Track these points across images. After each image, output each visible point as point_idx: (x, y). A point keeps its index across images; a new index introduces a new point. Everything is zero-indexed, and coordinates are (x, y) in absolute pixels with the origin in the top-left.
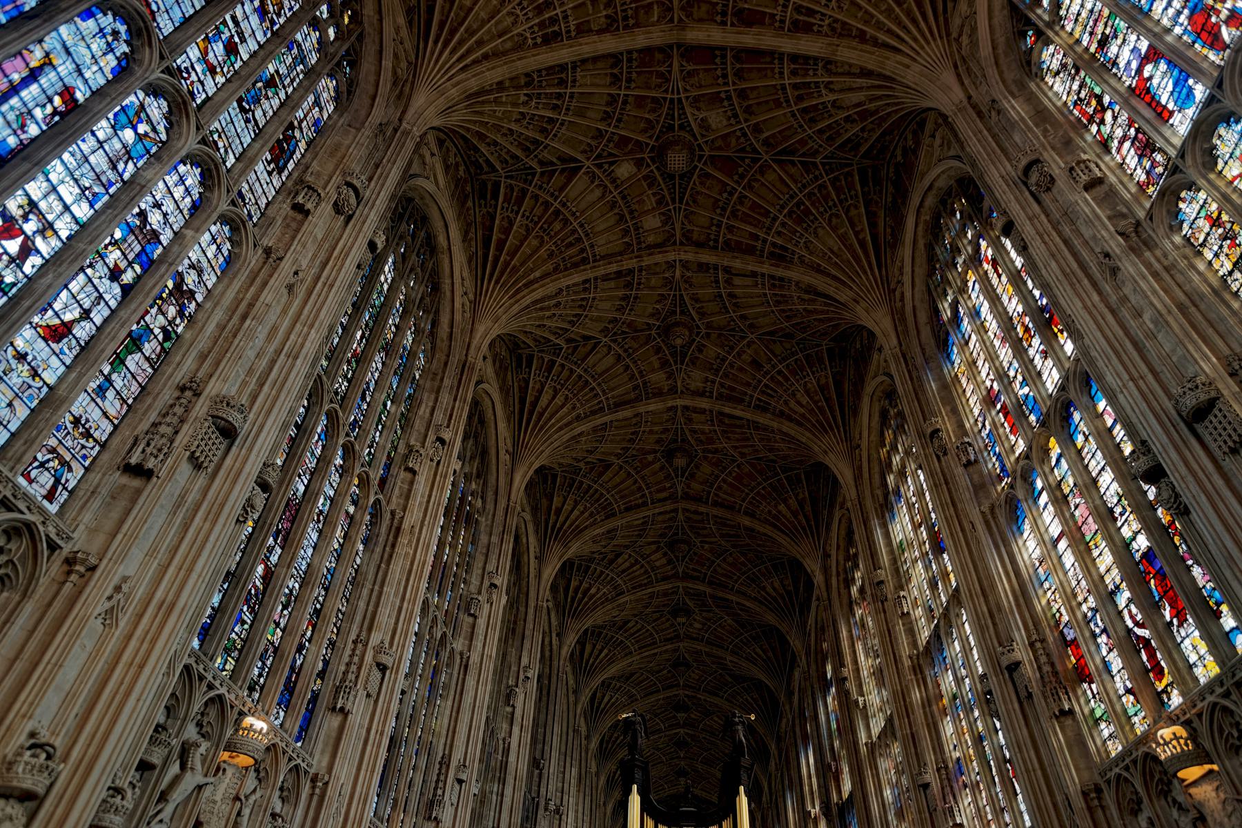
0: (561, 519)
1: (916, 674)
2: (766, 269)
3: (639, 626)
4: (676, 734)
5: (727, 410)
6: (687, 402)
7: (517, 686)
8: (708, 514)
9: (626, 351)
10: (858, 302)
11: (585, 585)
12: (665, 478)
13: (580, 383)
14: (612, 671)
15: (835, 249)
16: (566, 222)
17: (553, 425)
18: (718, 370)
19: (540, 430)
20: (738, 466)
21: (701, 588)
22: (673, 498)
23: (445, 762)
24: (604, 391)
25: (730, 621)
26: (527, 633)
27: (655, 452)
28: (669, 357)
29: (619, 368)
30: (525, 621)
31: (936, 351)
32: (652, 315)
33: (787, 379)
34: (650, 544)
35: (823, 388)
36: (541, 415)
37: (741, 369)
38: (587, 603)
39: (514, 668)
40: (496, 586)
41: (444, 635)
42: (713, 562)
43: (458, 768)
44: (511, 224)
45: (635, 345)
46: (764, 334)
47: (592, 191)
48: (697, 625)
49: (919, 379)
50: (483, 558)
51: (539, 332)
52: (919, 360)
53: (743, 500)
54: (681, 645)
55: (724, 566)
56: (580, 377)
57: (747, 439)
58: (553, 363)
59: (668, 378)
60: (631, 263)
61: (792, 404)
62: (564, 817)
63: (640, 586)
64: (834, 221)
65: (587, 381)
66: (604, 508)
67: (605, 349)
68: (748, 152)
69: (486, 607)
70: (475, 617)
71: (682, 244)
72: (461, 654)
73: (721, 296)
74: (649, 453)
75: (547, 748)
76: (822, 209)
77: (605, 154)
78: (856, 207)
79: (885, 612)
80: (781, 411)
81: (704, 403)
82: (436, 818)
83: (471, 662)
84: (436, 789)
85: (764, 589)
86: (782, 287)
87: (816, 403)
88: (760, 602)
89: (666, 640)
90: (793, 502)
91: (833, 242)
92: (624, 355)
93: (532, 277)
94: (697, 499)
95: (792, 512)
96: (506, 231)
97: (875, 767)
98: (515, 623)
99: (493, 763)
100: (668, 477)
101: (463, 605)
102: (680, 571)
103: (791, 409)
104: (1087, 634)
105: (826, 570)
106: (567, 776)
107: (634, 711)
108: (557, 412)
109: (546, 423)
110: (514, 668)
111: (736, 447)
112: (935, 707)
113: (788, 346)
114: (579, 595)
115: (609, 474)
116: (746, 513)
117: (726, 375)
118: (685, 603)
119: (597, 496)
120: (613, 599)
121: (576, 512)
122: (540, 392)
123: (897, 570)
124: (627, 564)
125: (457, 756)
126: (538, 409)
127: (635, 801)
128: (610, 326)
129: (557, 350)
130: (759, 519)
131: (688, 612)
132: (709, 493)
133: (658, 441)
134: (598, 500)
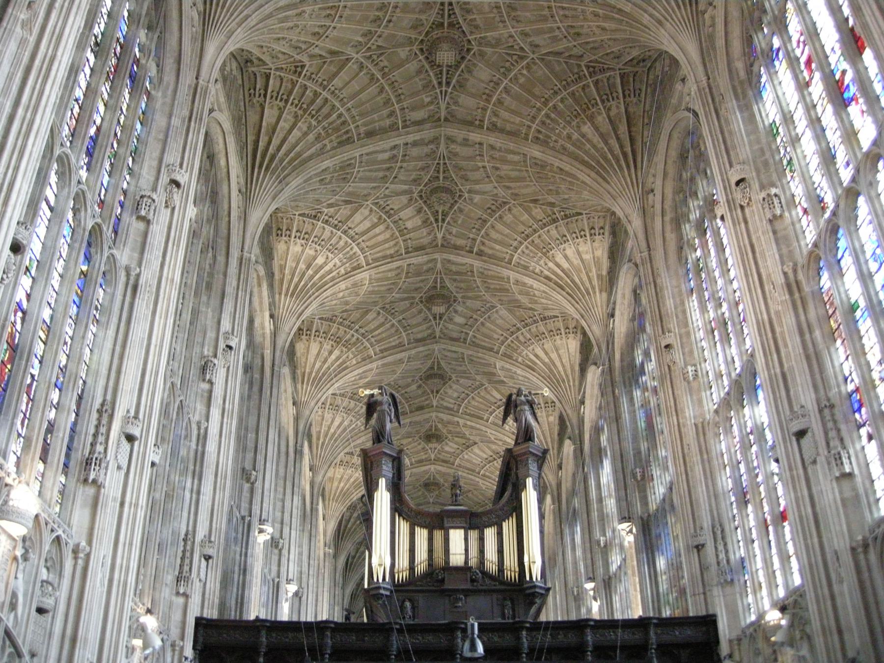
0: (275, 142)
1: (791, 293)
3: (381, 319)
4: (426, 472)
7: (215, 356)
8: (481, 144)
11: (310, 252)
12: (425, 87)
20: (528, 67)
22: (435, 120)
23: (106, 411)
25: (504, 312)
26: (230, 290)
27: (410, 42)
30: (225, 275)
38: (312, 277)
39: (211, 335)
40: (178, 184)
41: (96, 231)
42: (485, 221)
43: (126, 420)
48: (459, 320)
50: (159, 146)
53: (534, 118)
54: (436, 347)
55: (499, 226)
57: (544, 19)
62: (285, 552)
63: (385, 257)
66: (337, 130)
69: (165, 214)
70: (148, 222)
72: (128, 270)
74: (402, 45)
75: (260, 458)
79: (746, 222)
82: (94, 481)
83: (142, 281)
84: (93, 445)
89: (418, 341)
90: (601, 119)
94: (469, 123)
95: (602, 136)
97: (704, 450)
98: (211, 275)
99: (183, 452)
100: (427, 86)
101: (128, 204)
102: (440, 236)
106: (288, 504)
107: (380, 388)
110: (211, 335)
111: (526, 35)
112: (817, 333)
115: (344, 75)
119: (325, 110)
120: (347, 275)
121: (296, 133)
123: (766, 164)
124: (367, 224)
125: (125, 404)
127: (383, 499)
130: (553, 149)
132: (484, 109)
133: (414, 27)
134: (328, 115)
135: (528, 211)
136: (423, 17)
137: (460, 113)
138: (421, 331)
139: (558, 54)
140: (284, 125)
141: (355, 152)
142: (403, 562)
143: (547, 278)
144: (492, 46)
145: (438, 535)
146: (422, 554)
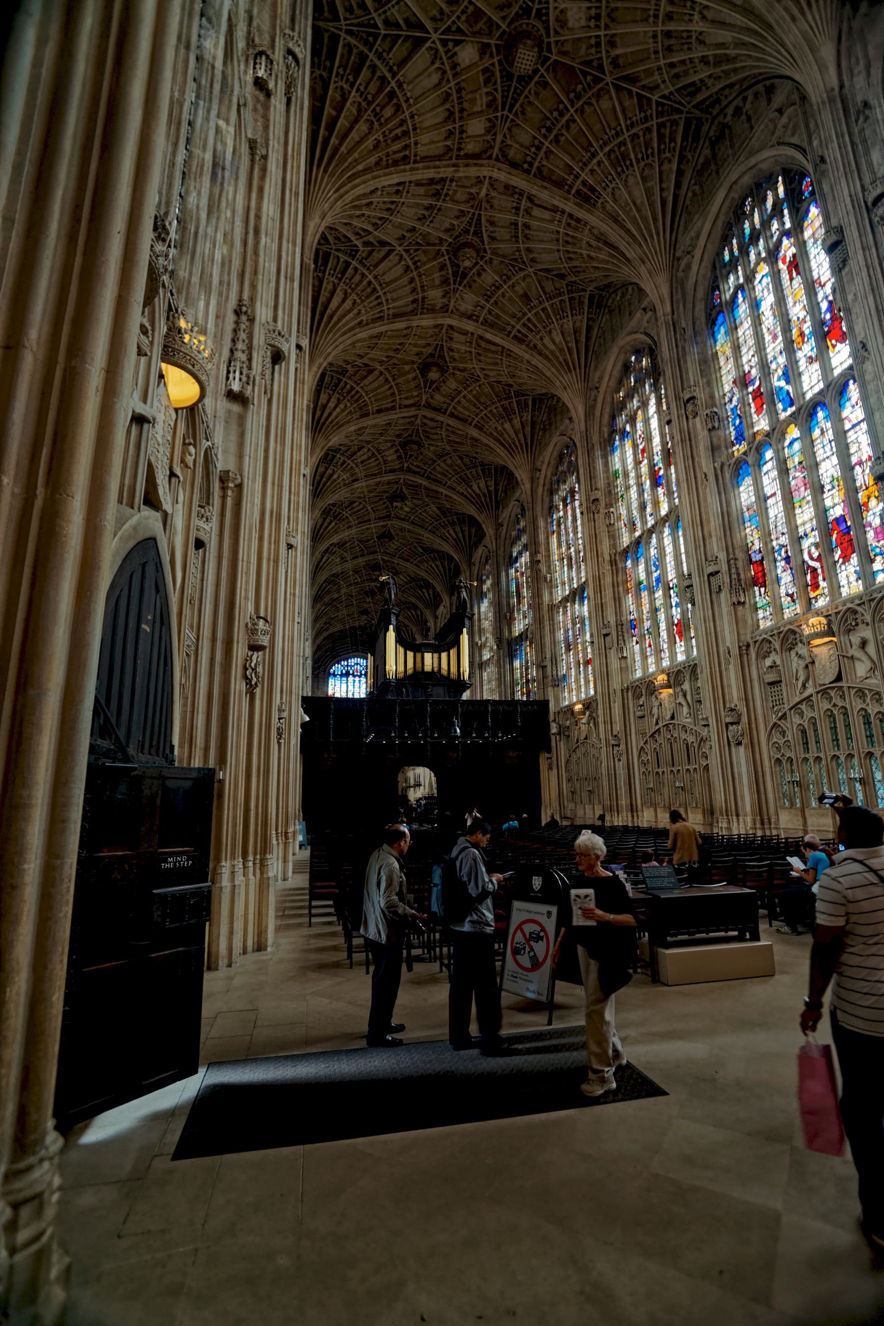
0: (325, 415)
2: (570, 207)
5: (488, 336)
6: (454, 322)
9: (415, 263)
10: (644, 263)
13: (369, 290)
14: (335, 539)
15: (638, 202)
16: (398, 107)
17: (340, 329)
18: (490, 297)
19: (330, 331)
21: (420, 481)
24: (387, 300)
25: (434, 509)
27: (413, 362)
28: (450, 276)
29: (406, 280)
31: (704, 326)
32: (447, 230)
33: (548, 317)
34: (386, 441)
35: (576, 332)
36: (331, 317)
37: (511, 299)
44: (344, 99)
45: (425, 259)
46: (540, 270)
47: (429, 75)
48: (407, 509)
49: (684, 348)
51: (343, 230)
52: (690, 332)
53: (477, 415)
55: (442, 465)
56: (370, 283)
58: (347, 264)
59: (444, 296)
60: (447, 172)
61: (547, 340)
64: (647, 171)
65: (374, 289)
66: (360, 409)
67: (397, 258)
68: (592, 67)
71: (497, 159)
73: (516, 225)
74: (407, 364)
76: (640, 156)
77: (454, 28)
78: (670, 161)
80: (535, 346)
81: (469, 326)
85: (471, 487)
86: (576, 229)
87: (567, 343)
88: (466, 497)
89: (380, 518)
90: (517, 422)
91: (639, 194)
92: (412, 267)
93: (354, 171)
96: (339, 108)
97: (552, 619)
103: (544, 345)
104: (771, 558)
105: (532, 480)
108: (344, 316)
109: (334, 326)
112: (621, 588)
113: (558, 286)
114: (324, 479)
115: (370, 378)
116: (476, 426)
117: (496, 303)
118: (401, 491)
119: (357, 397)
121: (338, 410)
122: (333, 293)
123: (610, 492)
124: (365, 457)
126: (329, 312)
128: (408, 235)
129: (353, 252)
131: (402, 498)
134: (357, 401)
135: (461, 458)
136: (424, 350)
137: (434, 403)
138: (384, 513)
139: (499, 382)
140: (331, 405)
141: (369, 422)
142: (401, 669)
143: (466, 497)
144: (460, 370)
145: (419, 655)
146: (410, 665)
